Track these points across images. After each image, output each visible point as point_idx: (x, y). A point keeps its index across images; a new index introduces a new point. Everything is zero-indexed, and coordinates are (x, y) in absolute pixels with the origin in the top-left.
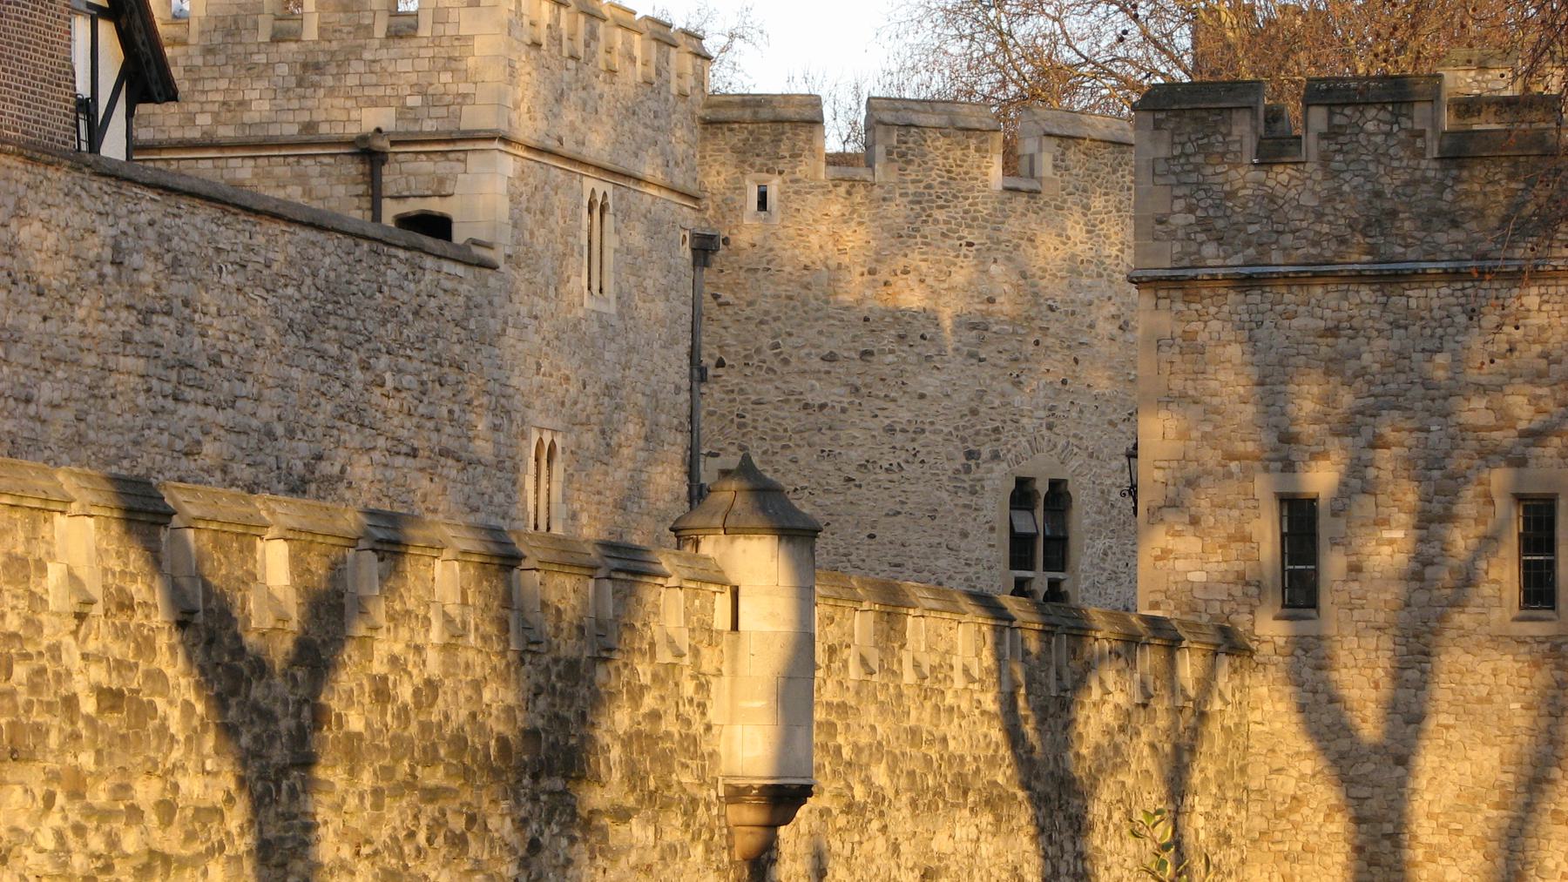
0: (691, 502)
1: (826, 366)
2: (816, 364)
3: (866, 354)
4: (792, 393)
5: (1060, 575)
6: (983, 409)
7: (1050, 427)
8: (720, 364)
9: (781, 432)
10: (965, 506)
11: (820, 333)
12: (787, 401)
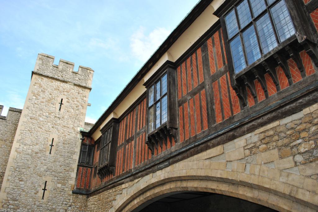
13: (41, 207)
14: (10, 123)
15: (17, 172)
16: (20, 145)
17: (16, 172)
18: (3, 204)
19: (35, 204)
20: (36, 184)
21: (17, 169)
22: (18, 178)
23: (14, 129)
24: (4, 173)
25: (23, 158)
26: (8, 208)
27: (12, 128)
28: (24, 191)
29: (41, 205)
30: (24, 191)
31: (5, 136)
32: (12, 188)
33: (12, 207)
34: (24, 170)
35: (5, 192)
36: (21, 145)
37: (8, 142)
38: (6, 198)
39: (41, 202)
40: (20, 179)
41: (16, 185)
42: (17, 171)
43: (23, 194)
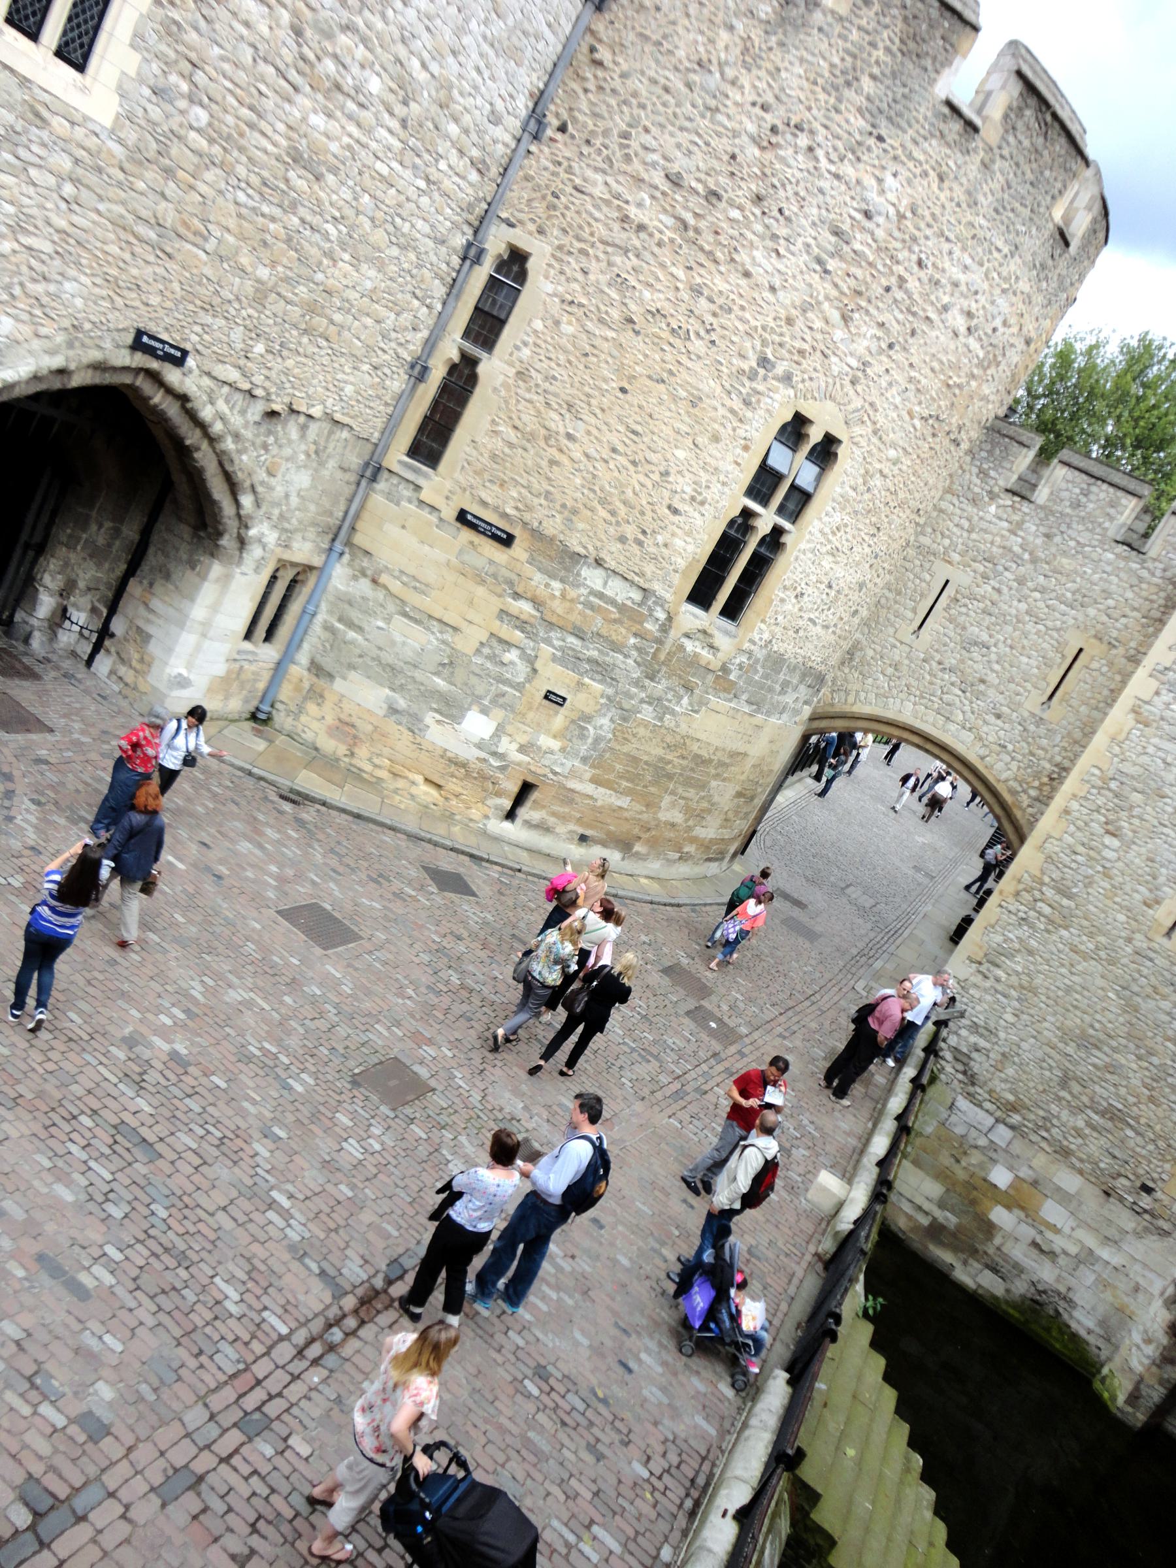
0: (464, 259)
1: (665, 186)
2: (658, 178)
3: (713, 196)
4: (618, 197)
5: (787, 525)
6: (800, 323)
7: (853, 383)
8: (562, 129)
9: (586, 236)
10: (732, 411)
11: (679, 146)
12: (607, 203)
13: (1149, 964)
14: (1158, 573)
15: (1111, 795)
16: (1157, 693)
17: (1106, 792)
18: (1021, 887)
19: (1129, 940)
20: (1163, 871)
21: (1113, 785)
22: (1103, 819)
23: (1162, 602)
24: (1067, 770)
25: (1151, 750)
26: (1034, 909)
27: (1154, 597)
28: (1107, 875)
29: (1152, 955)
30: (1107, 875)
31: (1118, 625)
32: (1070, 846)
33: (1047, 910)
34: (1136, 798)
35: (1041, 848)
36: (1164, 692)
37: (1121, 650)
38: (1038, 873)
39: (1157, 946)
40: (1110, 827)
41: (1085, 840)
42: (1109, 789)
43: (1102, 883)
